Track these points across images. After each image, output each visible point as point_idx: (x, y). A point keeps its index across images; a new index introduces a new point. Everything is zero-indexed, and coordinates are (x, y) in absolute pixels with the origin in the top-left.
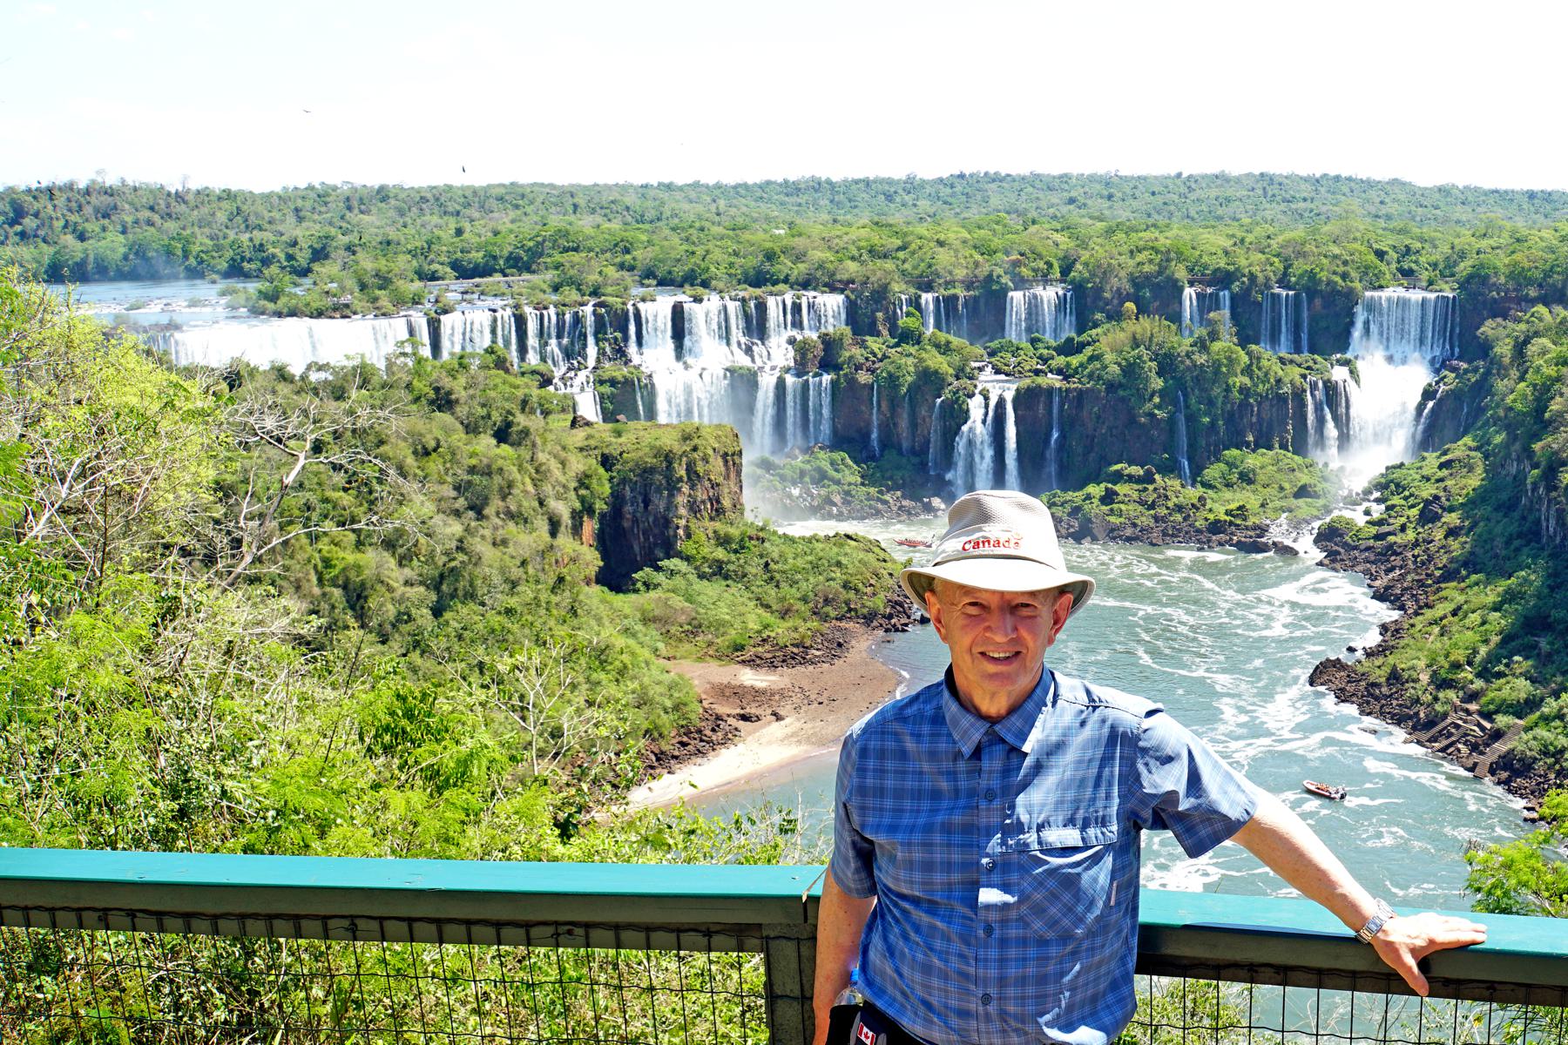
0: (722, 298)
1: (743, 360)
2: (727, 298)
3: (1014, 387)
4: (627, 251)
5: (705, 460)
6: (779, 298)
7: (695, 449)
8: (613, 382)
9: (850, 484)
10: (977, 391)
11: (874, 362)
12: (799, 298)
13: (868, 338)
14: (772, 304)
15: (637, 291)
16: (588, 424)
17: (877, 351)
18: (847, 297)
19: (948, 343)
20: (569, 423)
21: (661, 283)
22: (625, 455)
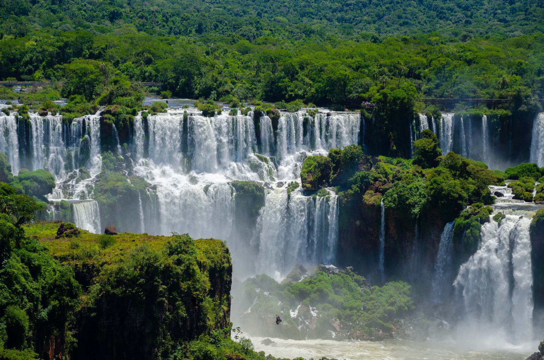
0: (234, 113)
1: (252, 176)
2: (239, 112)
3: (533, 213)
4: (148, 62)
5: (189, 274)
6: (291, 115)
7: (179, 262)
8: (114, 191)
9: (351, 309)
10: (491, 216)
11: (385, 182)
12: (312, 114)
13: (381, 157)
14: (283, 119)
15: (150, 101)
16: (76, 233)
17: (388, 171)
18: (362, 115)
19: (465, 165)
20: (55, 232)
21: (177, 94)
22: (106, 267)
